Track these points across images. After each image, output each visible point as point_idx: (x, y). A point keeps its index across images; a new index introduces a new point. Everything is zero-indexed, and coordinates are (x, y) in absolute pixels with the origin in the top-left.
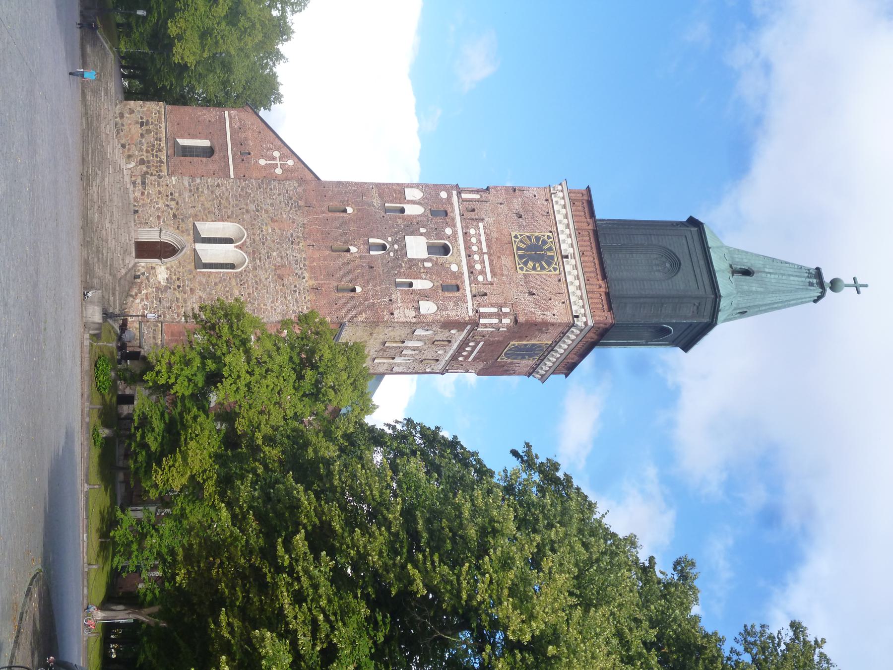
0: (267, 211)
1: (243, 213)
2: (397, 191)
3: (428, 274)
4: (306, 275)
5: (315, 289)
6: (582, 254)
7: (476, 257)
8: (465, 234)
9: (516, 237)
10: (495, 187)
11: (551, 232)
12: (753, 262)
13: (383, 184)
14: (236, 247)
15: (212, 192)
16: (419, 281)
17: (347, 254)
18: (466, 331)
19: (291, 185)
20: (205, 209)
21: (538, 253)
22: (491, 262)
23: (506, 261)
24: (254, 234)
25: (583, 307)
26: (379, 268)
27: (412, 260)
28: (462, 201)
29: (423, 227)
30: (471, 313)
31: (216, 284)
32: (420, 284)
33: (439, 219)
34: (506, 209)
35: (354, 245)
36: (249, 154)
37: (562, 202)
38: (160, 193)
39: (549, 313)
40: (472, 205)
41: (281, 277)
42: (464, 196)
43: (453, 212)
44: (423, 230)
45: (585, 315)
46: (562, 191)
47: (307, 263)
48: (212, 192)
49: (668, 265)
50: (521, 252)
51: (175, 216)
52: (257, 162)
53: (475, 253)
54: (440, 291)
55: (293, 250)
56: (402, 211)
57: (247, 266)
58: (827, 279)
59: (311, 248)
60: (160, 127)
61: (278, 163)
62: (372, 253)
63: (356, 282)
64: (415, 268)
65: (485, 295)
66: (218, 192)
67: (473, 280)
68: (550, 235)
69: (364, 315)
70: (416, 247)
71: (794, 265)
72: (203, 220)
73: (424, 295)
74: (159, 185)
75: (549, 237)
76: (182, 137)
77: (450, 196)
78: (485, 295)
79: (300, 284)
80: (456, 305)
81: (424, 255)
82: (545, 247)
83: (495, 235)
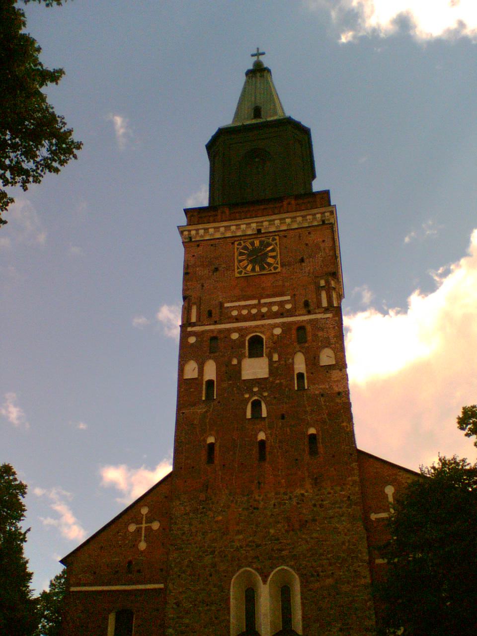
4: (299, 491)
5: (317, 481)
7: (264, 310)
8: (237, 319)
9: (240, 273)
11: (233, 243)
13: (178, 401)
14: (265, 582)
15: (187, 612)
16: (296, 366)
17: (268, 444)
22: (269, 296)
28: (199, 322)
29: (230, 361)
30: (329, 315)
32: (300, 364)
35: (256, 435)
36: (130, 563)
39: (322, 245)
41: (303, 524)
42: (194, 319)
43: (212, 331)
44: (235, 362)
45: (323, 213)
47: (282, 490)
48: (187, 612)
50: (257, 268)
52: (142, 552)
53: (259, 311)
54: (307, 345)
56: (210, 383)
57: (292, 567)
61: (144, 525)
62: (264, 414)
65: (306, 304)
67: (290, 313)
69: (344, 424)
70: (255, 369)
73: (312, 362)
75: (240, 244)
82: (250, 247)
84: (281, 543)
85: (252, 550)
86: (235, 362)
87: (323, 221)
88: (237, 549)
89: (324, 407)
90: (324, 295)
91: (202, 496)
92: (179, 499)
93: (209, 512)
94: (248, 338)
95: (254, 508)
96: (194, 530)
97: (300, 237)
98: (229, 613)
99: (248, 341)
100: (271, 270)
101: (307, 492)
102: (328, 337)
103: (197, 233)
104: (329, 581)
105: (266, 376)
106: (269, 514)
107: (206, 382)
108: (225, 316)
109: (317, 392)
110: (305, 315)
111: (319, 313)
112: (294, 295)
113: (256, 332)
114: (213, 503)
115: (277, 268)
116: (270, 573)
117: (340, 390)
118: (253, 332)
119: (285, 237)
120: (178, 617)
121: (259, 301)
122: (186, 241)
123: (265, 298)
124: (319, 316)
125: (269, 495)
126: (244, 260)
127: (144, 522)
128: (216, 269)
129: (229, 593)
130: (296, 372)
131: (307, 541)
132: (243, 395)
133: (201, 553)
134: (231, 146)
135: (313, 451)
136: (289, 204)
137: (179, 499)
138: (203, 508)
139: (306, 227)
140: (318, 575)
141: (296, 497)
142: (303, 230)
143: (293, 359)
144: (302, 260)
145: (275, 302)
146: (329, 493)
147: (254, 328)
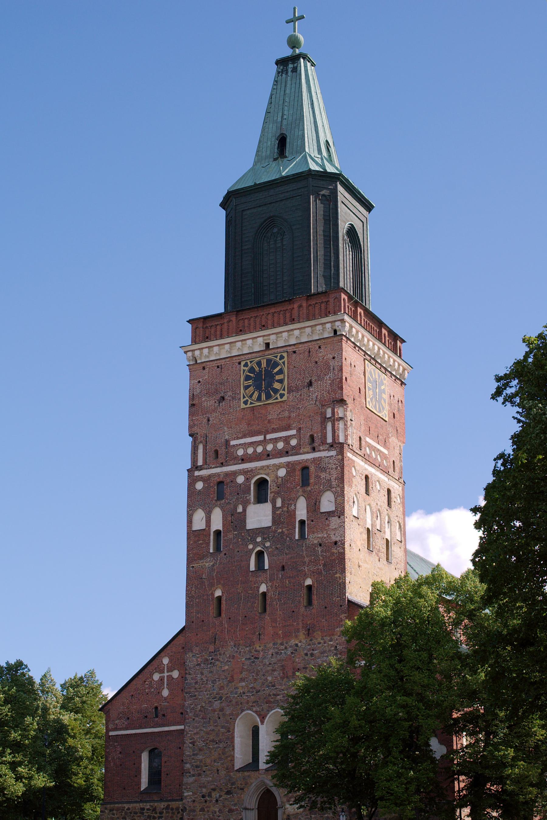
0: (221, 688)
1: (224, 715)
2: (195, 538)
3: (290, 502)
4: (293, 642)
5: (309, 632)
6: (264, 327)
7: (270, 447)
8: (243, 460)
9: (246, 403)
10: (190, 427)
11: (240, 363)
12: (270, 135)
13: (188, 555)
14: (262, 723)
15: (201, 750)
16: (297, 513)
17: (268, 595)
18: (354, 458)
19: (191, 660)
20: (220, 759)
21: (263, 377)
22: (274, 431)
24: (248, 702)
27: (274, 521)
29: (236, 508)
30: (333, 453)
32: (301, 511)
33: (227, 490)
34: (214, 414)
35: (258, 588)
36: (156, 708)
37: (206, 351)
38: (202, 810)
39: (332, 363)
40: (212, 454)
42: (200, 462)
43: (218, 475)
44: (240, 509)
46: (193, 351)
47: (279, 642)
48: (201, 750)
49: (275, 230)
50: (263, 397)
51: (228, 793)
52: (166, 699)
53: (265, 449)
54: (309, 488)
55: (265, 658)
56: (218, 533)
58: (288, 52)
59: (262, 637)
60: (128, 809)
61: (166, 674)
62: (266, 567)
63: (301, 585)
64: (283, 517)
65: (312, 437)
66: (200, 744)
67: (296, 450)
68: (243, 363)
69: (338, 575)
70: (259, 516)
71: (273, 89)
72: (233, 760)
73: (314, 507)
74: (194, 811)
75: (246, 365)
76: (139, 783)
77: (201, 478)
78: (312, 437)
79: (303, 650)
80: (324, 470)
81: (267, 507)
82: (257, 369)
83: (244, 427)
85: (253, 695)
87: (335, 332)
88: (241, 695)
89: (321, 558)
91: (211, 648)
92: (192, 651)
93: (217, 663)
94: (253, 481)
95: (256, 658)
96: (204, 679)
97: (309, 352)
98: (233, 749)
99: (254, 483)
100: (277, 398)
101: (300, 642)
102: (331, 480)
103: (201, 353)
105: (270, 524)
106: (268, 663)
107: (214, 532)
109: (316, 542)
110: (309, 453)
111: (324, 450)
112: (300, 428)
113: (261, 474)
114: (220, 654)
115: (284, 395)
116: (266, 716)
117: (337, 539)
118: (258, 474)
120: (194, 755)
121: (265, 437)
122: (191, 363)
123: (271, 433)
125: (268, 646)
126: (249, 386)
127: (166, 671)
129: (233, 733)
132: (247, 546)
133: (210, 700)
134: (244, 213)
135: (310, 602)
136: (300, 306)
137: (192, 651)
138: (212, 659)
139: (316, 340)
141: (291, 647)
143: (295, 505)
144: (310, 384)
145: (281, 438)
146: (319, 643)
147: (259, 470)
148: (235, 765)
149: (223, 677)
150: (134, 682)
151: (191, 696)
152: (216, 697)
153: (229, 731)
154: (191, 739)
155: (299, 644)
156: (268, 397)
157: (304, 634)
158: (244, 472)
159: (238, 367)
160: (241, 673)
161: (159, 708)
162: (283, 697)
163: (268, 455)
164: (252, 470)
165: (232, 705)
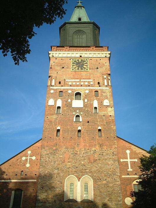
0: (58, 164)
1: (60, 176)
3: (90, 100)
5: (101, 146)
7: (82, 83)
9: (73, 70)
14: (79, 181)
22: (83, 79)
23: (84, 74)
25: (102, 54)
26: (89, 119)
30: (108, 88)
31: (101, 192)
32: (96, 104)
33: (64, 94)
34: (60, 72)
39: (105, 64)
43: (61, 89)
44: (69, 101)
47: (87, 148)
50: (80, 69)
52: (28, 168)
54: (98, 97)
55: (80, 154)
56: (59, 108)
57: (90, 176)
61: (29, 158)
62: (81, 120)
65: (99, 83)
67: (92, 86)
68: (72, 59)
69: (112, 127)
70: (78, 104)
73: (101, 103)
77: (53, 89)
79: (99, 152)
83: (72, 76)
84: (86, 167)
86: (69, 101)
88: (68, 168)
90: (105, 81)
93: (57, 154)
96: (50, 160)
101: (97, 149)
104: (105, 182)
106: (82, 156)
108: (66, 84)
114: (59, 151)
116: (81, 178)
117: (111, 115)
119: (91, 59)
121: (80, 80)
124: (104, 88)
128: (63, 68)
129: (64, 184)
130: (94, 106)
131: (96, 167)
133: (53, 169)
138: (55, 152)
140: (100, 179)
141: (92, 151)
142: (98, 58)
144: (97, 68)
148: (65, 199)
149: (60, 160)
150: (12, 160)
151: (43, 167)
152: (55, 168)
153: (62, 184)
154: (41, 186)
155: (96, 150)
156: (82, 69)
157: (98, 146)
158: (72, 90)
159: (70, 60)
160: (69, 159)
161: (24, 171)
162: (89, 170)
163: (81, 86)
164: (75, 89)
165: (64, 172)
